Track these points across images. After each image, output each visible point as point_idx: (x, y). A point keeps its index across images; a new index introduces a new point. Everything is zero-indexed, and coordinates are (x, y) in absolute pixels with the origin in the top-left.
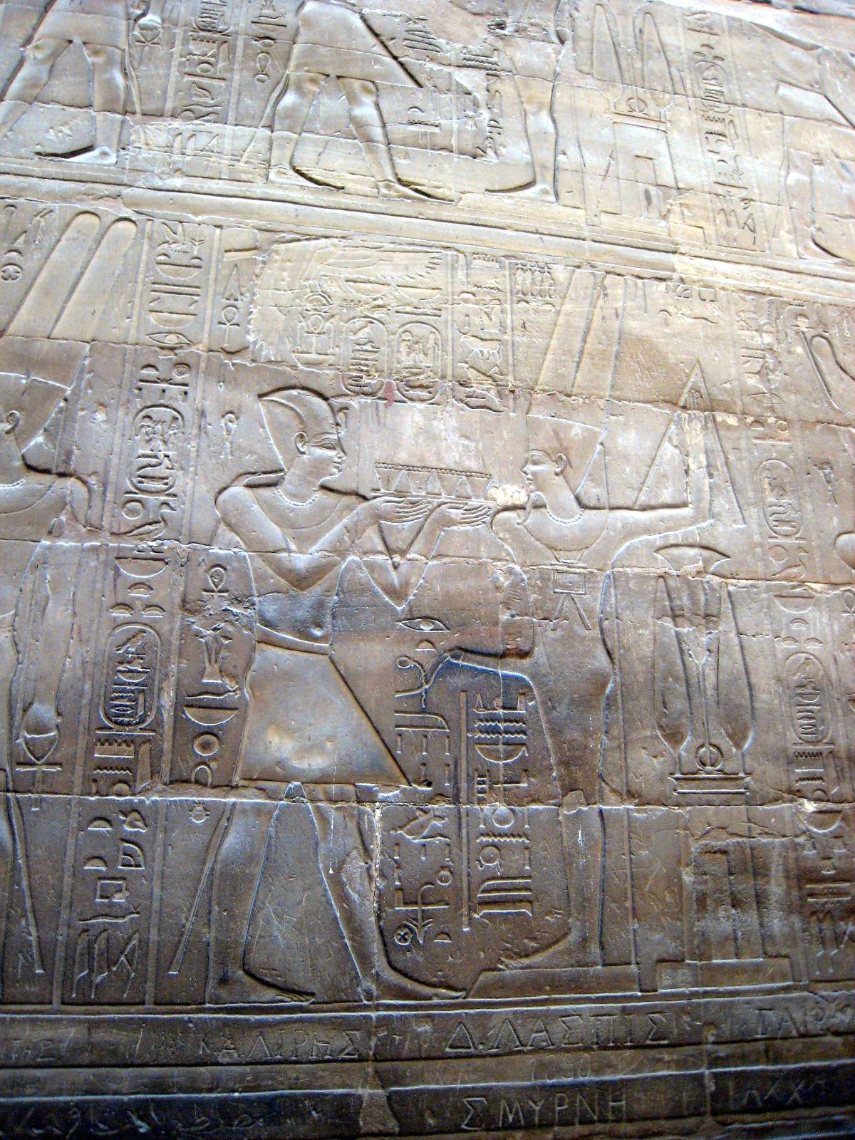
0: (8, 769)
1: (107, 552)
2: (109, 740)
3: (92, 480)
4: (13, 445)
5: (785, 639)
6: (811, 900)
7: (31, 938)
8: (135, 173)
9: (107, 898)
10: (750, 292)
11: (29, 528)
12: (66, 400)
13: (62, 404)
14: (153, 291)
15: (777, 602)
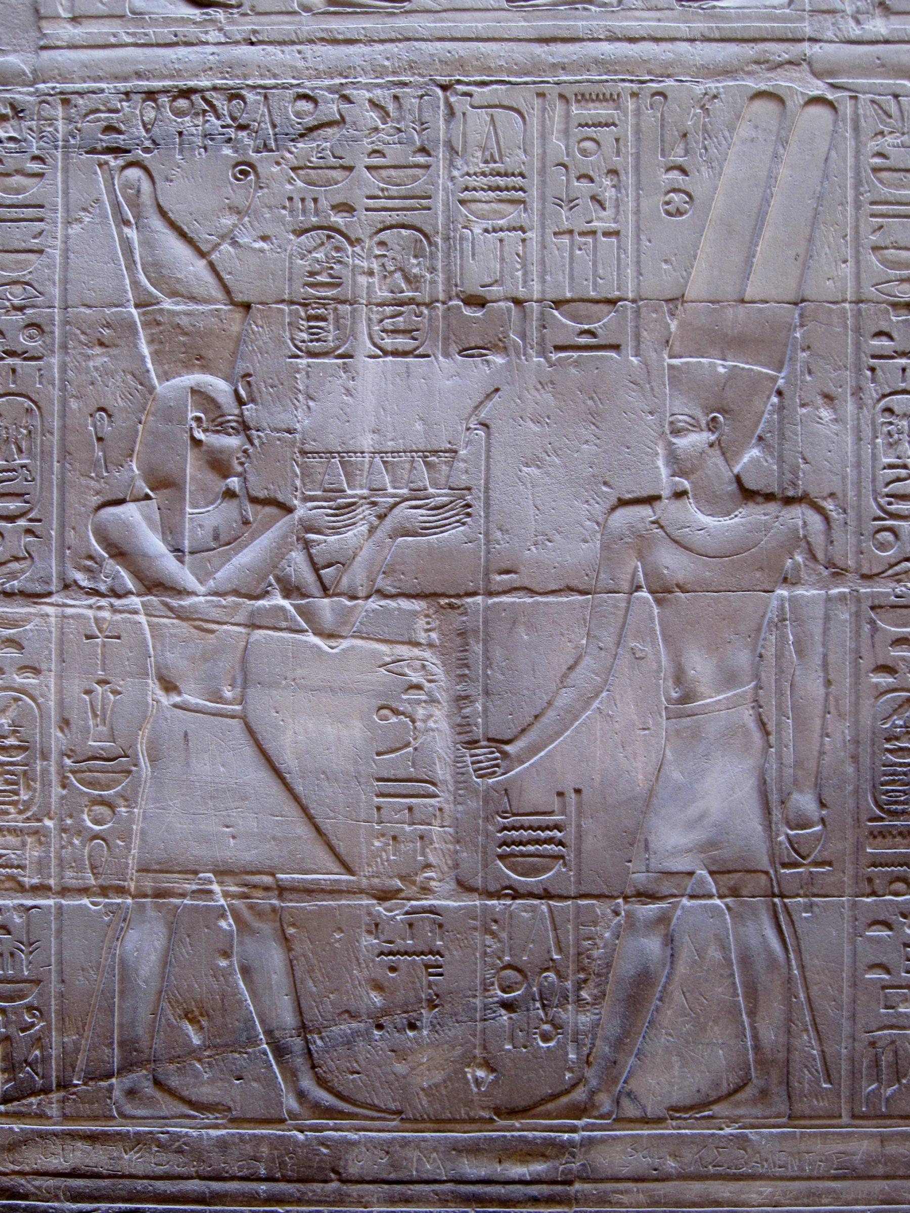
0: (771, 872)
1: (858, 600)
2: (882, 834)
3: (829, 505)
4: (720, 461)
7: (815, 1052)
8: (821, 17)
9: (893, 1008)
11: (758, 575)
12: (779, 393)
13: (775, 400)
14: (872, 216)
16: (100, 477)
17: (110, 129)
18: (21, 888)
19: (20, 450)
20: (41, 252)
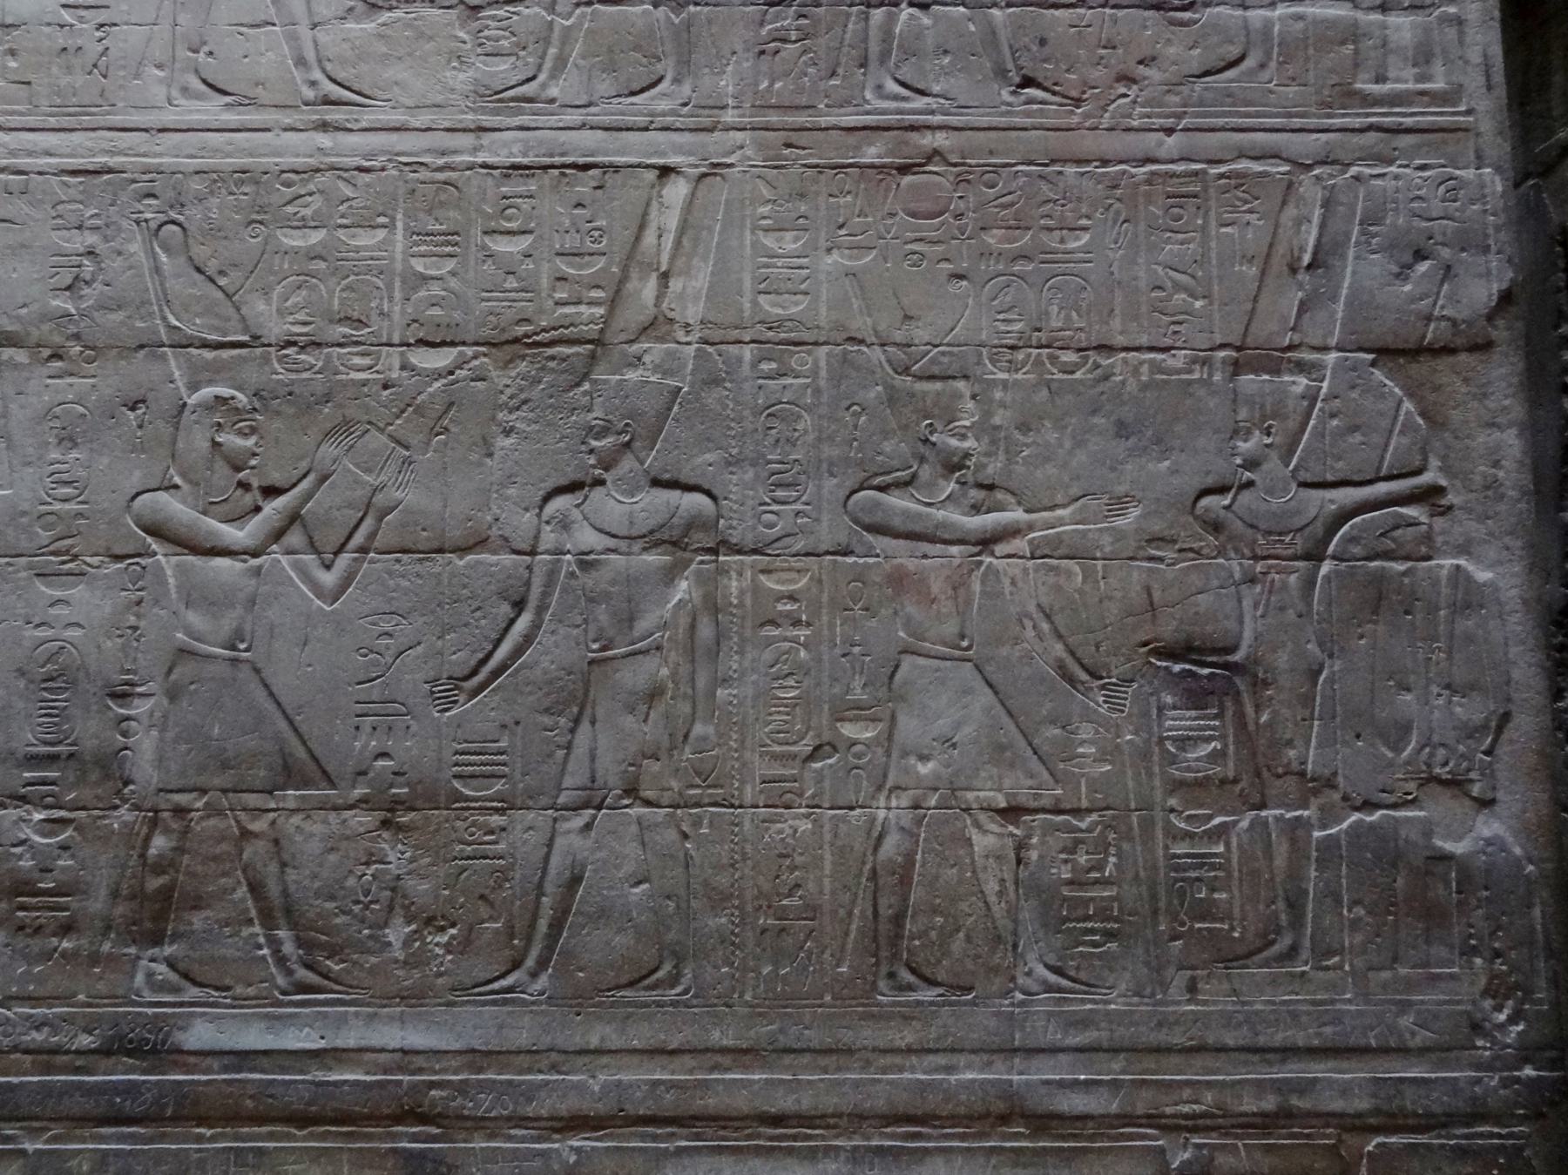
5: (38, 626)
6: (20, 914)
10: (74, 173)
15: (37, 582)
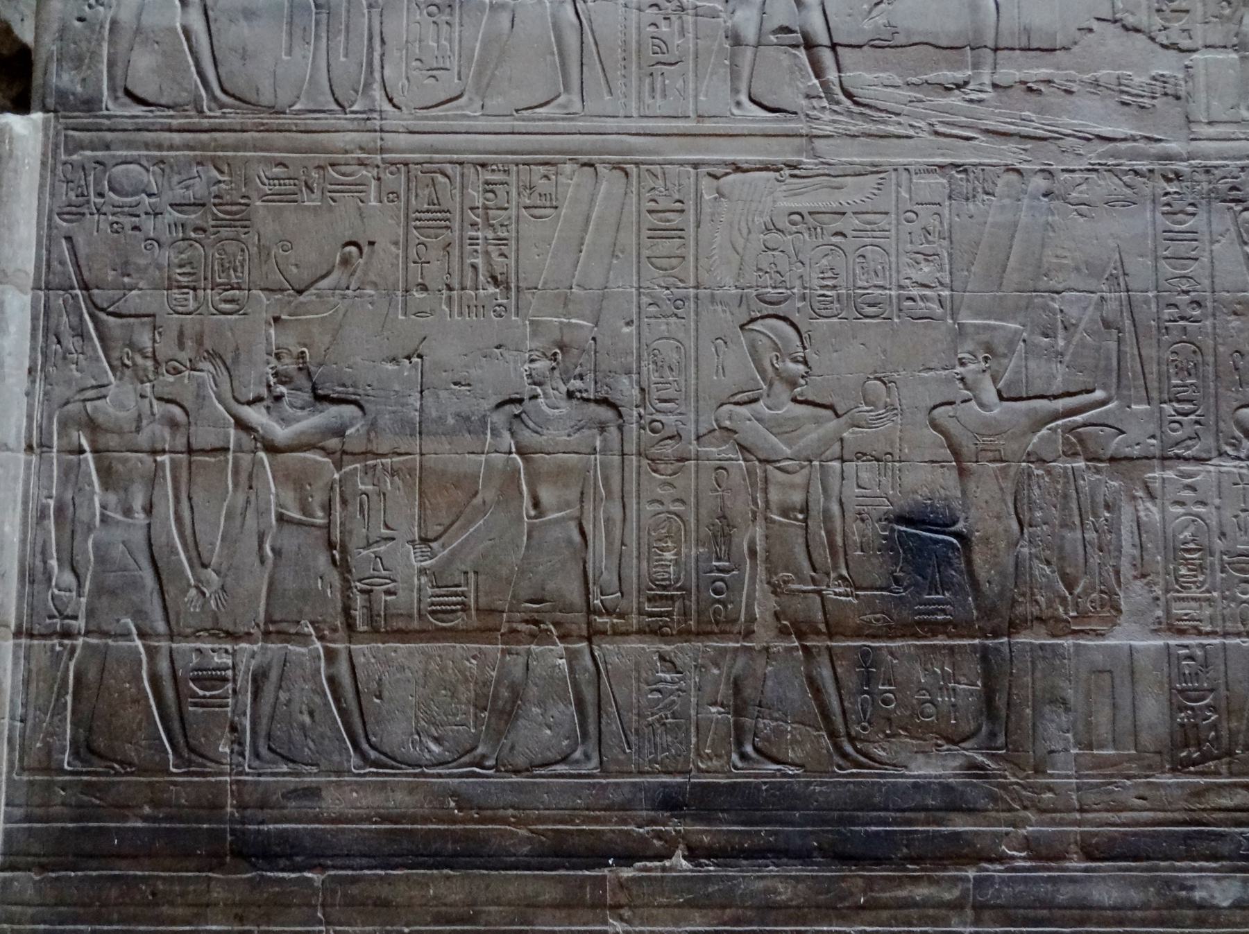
16: (1237, 391)
17: (1234, 188)
18: (1200, 633)
19: (1190, 374)
20: (1196, 259)
